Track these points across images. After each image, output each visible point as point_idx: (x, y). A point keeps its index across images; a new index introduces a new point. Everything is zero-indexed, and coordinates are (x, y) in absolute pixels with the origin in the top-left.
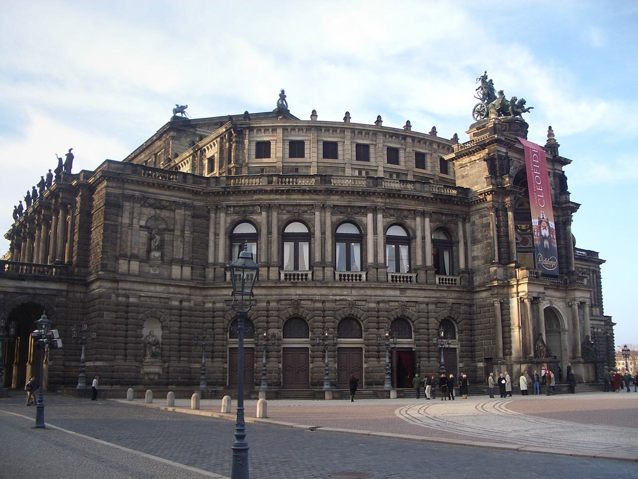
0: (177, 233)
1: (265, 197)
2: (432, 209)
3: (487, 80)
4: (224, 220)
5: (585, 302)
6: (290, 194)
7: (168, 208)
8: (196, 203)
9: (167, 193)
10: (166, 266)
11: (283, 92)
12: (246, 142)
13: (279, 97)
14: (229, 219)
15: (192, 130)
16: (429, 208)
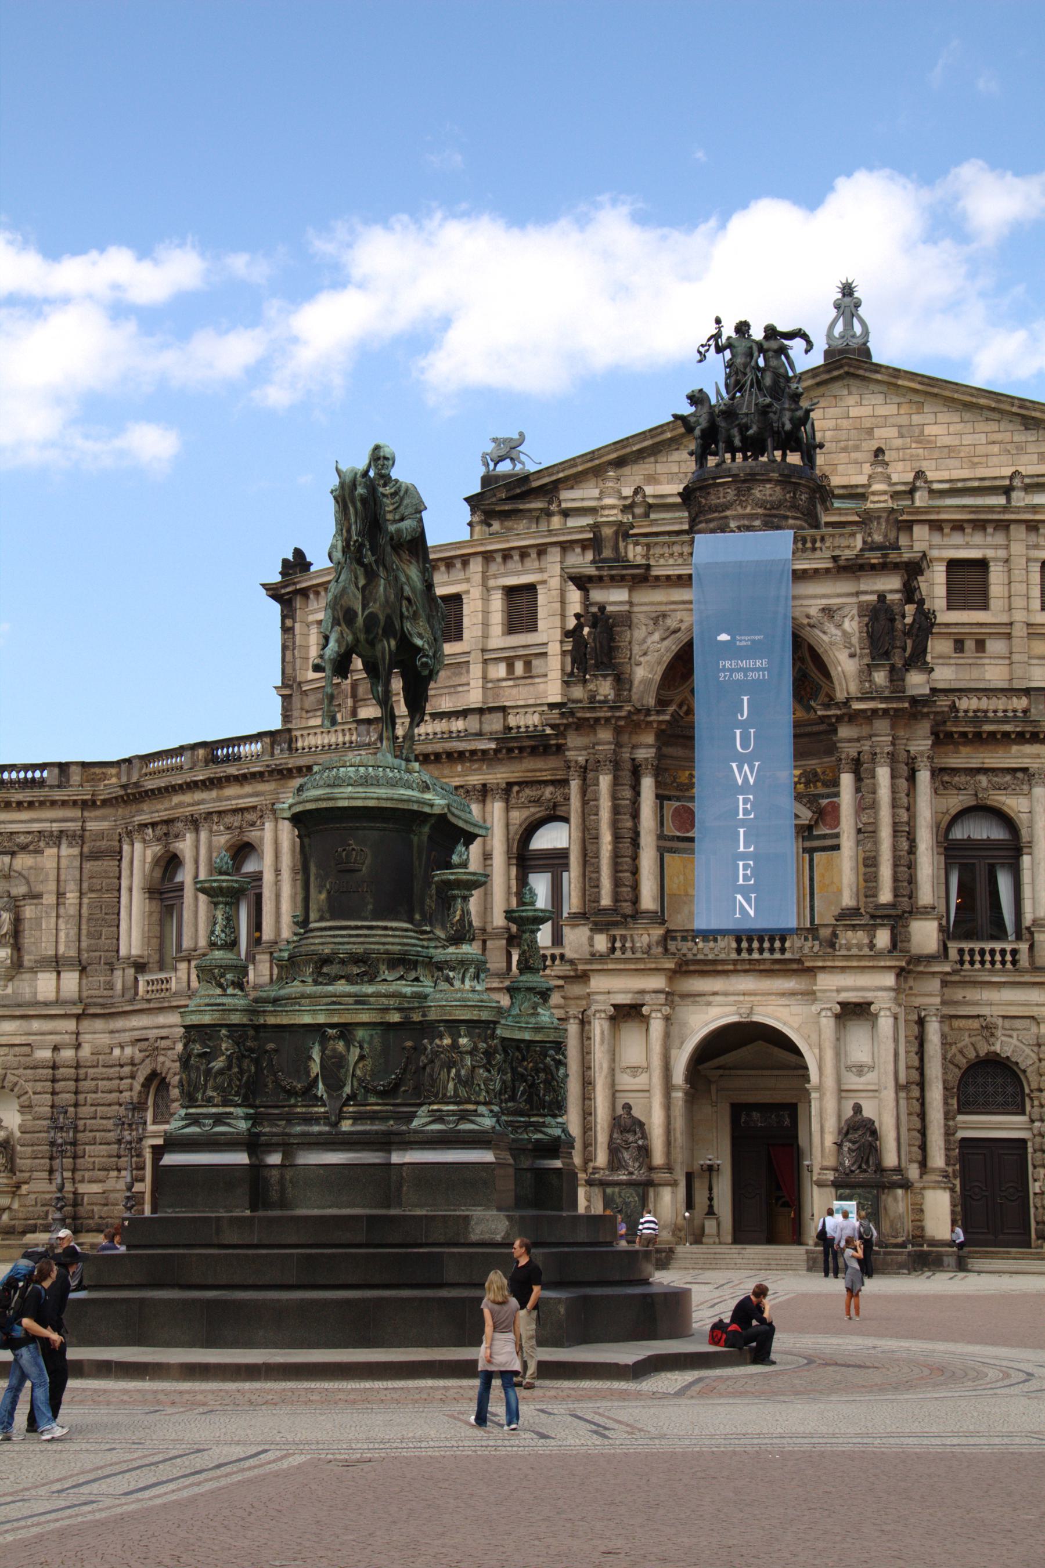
0: (49, 899)
1: (187, 798)
2: (504, 775)
3: (757, 334)
4: (140, 858)
5: (870, 1004)
6: (221, 788)
7: (31, 848)
8: (91, 826)
9: (25, 815)
10: (27, 976)
11: (847, 290)
12: (297, 626)
13: (834, 312)
14: (149, 853)
15: (538, 505)
16: (499, 776)
